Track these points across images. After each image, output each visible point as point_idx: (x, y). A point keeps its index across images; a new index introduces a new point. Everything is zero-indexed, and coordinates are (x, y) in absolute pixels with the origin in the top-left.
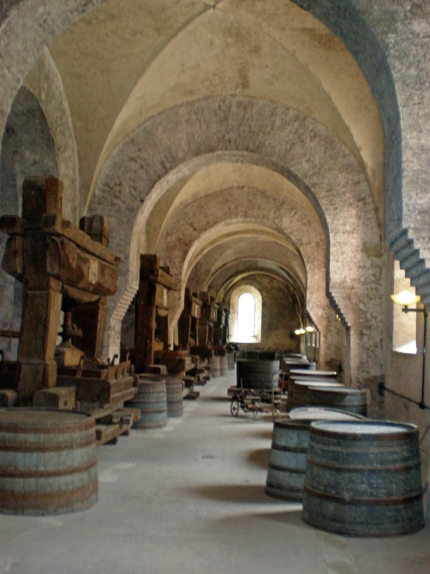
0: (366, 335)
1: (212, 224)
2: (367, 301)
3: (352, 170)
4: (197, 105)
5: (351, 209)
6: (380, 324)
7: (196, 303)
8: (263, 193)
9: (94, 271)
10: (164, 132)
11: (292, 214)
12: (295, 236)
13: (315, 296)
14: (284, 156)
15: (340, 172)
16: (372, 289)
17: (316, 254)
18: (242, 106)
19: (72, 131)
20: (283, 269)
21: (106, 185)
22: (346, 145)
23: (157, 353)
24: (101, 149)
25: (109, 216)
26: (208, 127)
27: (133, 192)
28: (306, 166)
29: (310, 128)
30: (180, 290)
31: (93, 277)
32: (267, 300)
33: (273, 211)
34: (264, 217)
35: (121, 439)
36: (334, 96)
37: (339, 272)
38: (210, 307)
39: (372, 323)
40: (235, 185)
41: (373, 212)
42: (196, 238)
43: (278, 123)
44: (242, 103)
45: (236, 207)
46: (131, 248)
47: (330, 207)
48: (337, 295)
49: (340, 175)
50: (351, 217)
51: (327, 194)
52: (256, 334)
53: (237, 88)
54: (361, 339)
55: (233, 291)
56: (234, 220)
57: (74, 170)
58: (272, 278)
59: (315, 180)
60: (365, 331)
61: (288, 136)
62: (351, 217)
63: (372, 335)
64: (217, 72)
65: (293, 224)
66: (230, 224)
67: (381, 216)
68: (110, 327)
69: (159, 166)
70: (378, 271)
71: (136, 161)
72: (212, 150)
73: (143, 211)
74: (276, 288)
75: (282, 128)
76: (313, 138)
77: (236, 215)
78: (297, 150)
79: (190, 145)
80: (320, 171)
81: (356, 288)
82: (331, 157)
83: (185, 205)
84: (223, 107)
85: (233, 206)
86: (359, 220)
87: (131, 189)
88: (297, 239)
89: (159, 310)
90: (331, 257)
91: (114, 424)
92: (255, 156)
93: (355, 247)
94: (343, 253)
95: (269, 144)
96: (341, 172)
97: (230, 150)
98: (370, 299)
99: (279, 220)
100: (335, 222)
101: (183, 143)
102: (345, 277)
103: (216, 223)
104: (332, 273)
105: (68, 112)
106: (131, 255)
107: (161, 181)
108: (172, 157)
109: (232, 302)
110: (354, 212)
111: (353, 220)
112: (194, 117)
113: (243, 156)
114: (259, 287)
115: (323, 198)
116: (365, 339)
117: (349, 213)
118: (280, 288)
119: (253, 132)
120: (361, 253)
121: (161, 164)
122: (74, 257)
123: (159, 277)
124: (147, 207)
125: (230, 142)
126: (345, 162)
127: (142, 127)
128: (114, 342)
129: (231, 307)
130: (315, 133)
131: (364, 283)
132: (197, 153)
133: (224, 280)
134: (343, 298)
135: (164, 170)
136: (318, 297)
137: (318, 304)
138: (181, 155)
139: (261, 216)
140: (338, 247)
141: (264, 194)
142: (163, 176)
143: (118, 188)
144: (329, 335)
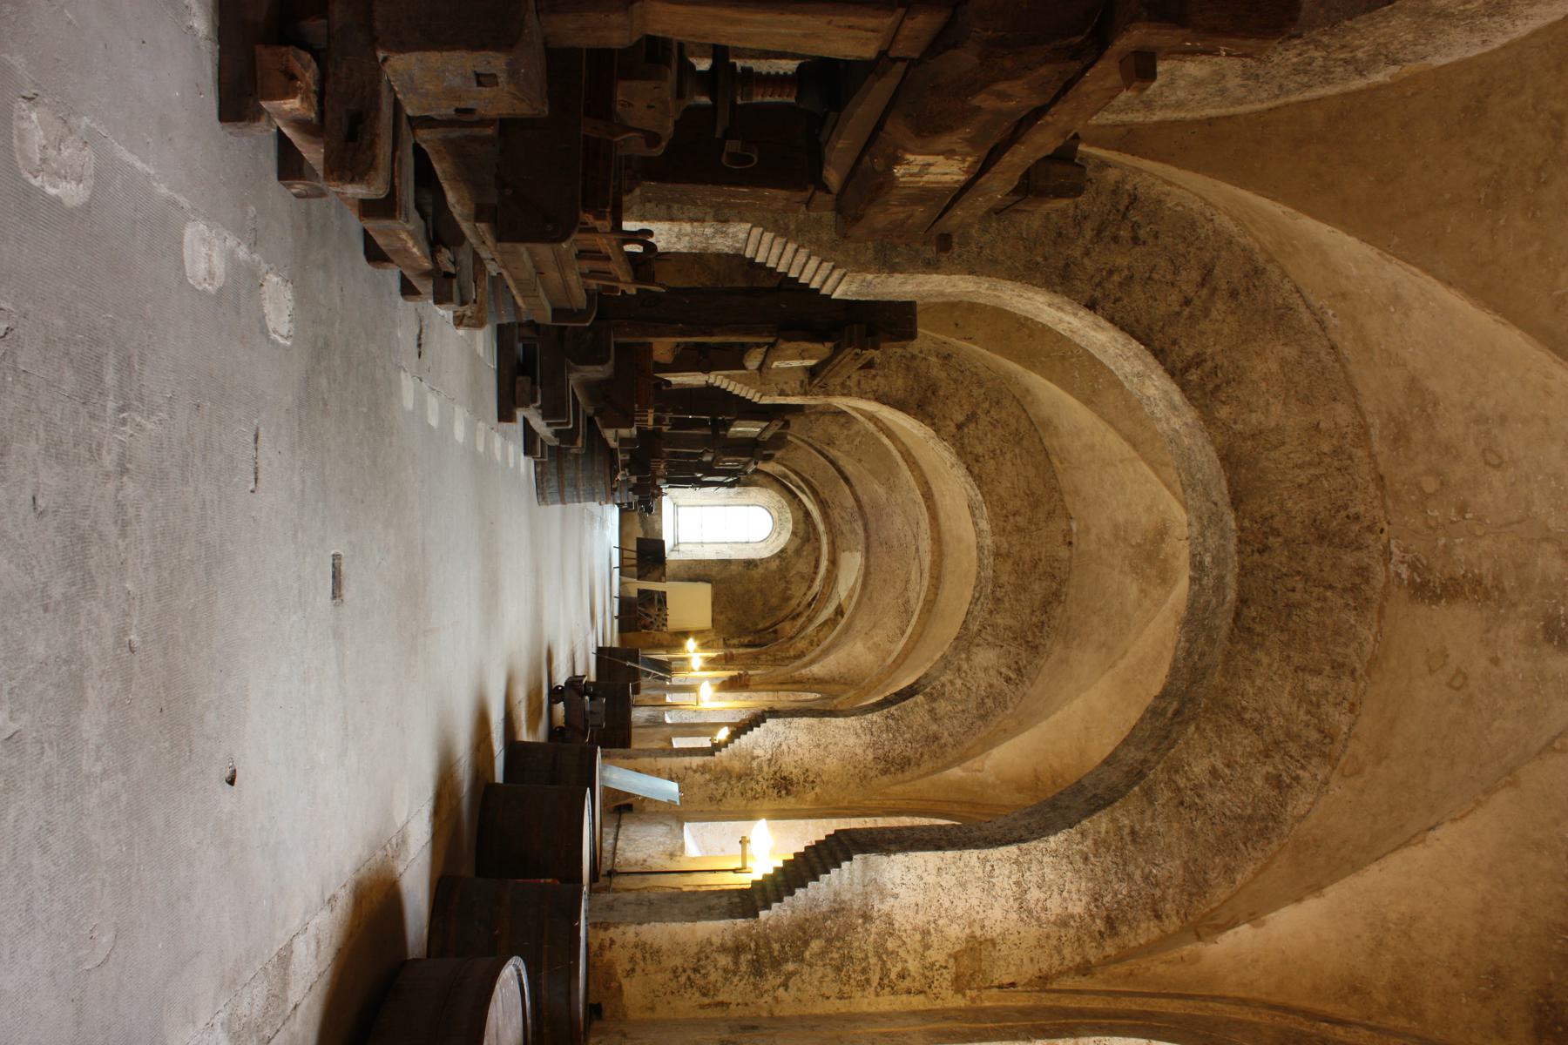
0: (736, 963)
1: (976, 470)
2: (832, 959)
3: (1191, 895)
4: (1360, 453)
5: (1085, 899)
6: (766, 998)
7: (764, 430)
8: (1057, 594)
9: (932, 169)
10: (1283, 362)
12: (952, 683)
13: (804, 738)
14: (1227, 706)
15: (1186, 863)
16: (864, 971)
17: (907, 736)
18: (1358, 580)
19: (1293, 98)
20: (839, 611)
21: (1134, 199)
22: (1256, 874)
23: (648, 349)
24: (1242, 185)
26: (1300, 486)
27: (1116, 278)
28: (1199, 769)
29: (1301, 772)
30: (805, 394)
31: (915, 170)
32: (761, 570)
33: (1012, 622)
34: (998, 600)
35: (390, 277)
36: (1419, 854)
37: (912, 876)
39: (770, 977)
40: (1074, 526)
41: (1078, 959)
42: (937, 431)
43: (1315, 684)
44: (1367, 581)
46: (956, 278)
47: (1089, 842)
48: (846, 875)
49: (1178, 862)
50: (1065, 900)
51: (1127, 830)
52: (681, 547)
53: (1413, 567)
54: (723, 949)
56: (984, 525)
57: (1180, 105)
58: (813, 581)
59: (1163, 795)
60: (745, 958)
61: (1280, 713)
62: (1065, 900)
63: (736, 980)
64: (1468, 516)
65: (982, 675)
66: (973, 515)
67: (1069, 983)
68: (726, 221)
69: (1190, 352)
70: (917, 984)
71: (1203, 284)
72: (1236, 502)
73: (1059, 309)
74: (790, 589)
75: (1302, 696)
76: (1275, 781)
77: (999, 531)
78: (1243, 742)
79: (1253, 436)
80: (1190, 807)
81: (867, 925)
82: (1226, 834)
83: (1021, 400)
84: (1355, 527)
86: (1055, 923)
87: (1126, 272)
88: (943, 685)
89: (763, 350)
90: (949, 854)
91: (433, 255)
92: (1224, 623)
93: (982, 915)
94: (963, 885)
95: (1258, 663)
96: (1185, 865)
97: (1239, 552)
98: (838, 969)
99: (990, 639)
100: (1047, 859)
101: (1254, 418)
102: (896, 896)
103: (978, 479)
104: (907, 859)
105: (1357, 84)
106: (936, 278)
107: (1150, 359)
108: (1218, 387)
109: (754, 492)
110: (1077, 908)
111: (1055, 905)
112: (1326, 448)
113: (1219, 586)
114: (790, 552)
115: (1113, 820)
116: (724, 961)
117: (1075, 897)
118: (789, 599)
119: (1289, 615)
120: (963, 936)
121: (1198, 355)
122: (1009, 97)
123: (858, 351)
124: (1068, 318)
125: (1260, 552)
126: (1212, 875)
127: (1294, 299)
128: (679, 237)
130: (1289, 787)
131: (881, 951)
132: (1229, 459)
134: (837, 894)
135: (1179, 365)
136: (800, 745)
137: (784, 747)
138: (1223, 412)
140: (980, 871)
141: (1054, 598)
142: (1163, 362)
143: (1124, 234)
144: (708, 776)
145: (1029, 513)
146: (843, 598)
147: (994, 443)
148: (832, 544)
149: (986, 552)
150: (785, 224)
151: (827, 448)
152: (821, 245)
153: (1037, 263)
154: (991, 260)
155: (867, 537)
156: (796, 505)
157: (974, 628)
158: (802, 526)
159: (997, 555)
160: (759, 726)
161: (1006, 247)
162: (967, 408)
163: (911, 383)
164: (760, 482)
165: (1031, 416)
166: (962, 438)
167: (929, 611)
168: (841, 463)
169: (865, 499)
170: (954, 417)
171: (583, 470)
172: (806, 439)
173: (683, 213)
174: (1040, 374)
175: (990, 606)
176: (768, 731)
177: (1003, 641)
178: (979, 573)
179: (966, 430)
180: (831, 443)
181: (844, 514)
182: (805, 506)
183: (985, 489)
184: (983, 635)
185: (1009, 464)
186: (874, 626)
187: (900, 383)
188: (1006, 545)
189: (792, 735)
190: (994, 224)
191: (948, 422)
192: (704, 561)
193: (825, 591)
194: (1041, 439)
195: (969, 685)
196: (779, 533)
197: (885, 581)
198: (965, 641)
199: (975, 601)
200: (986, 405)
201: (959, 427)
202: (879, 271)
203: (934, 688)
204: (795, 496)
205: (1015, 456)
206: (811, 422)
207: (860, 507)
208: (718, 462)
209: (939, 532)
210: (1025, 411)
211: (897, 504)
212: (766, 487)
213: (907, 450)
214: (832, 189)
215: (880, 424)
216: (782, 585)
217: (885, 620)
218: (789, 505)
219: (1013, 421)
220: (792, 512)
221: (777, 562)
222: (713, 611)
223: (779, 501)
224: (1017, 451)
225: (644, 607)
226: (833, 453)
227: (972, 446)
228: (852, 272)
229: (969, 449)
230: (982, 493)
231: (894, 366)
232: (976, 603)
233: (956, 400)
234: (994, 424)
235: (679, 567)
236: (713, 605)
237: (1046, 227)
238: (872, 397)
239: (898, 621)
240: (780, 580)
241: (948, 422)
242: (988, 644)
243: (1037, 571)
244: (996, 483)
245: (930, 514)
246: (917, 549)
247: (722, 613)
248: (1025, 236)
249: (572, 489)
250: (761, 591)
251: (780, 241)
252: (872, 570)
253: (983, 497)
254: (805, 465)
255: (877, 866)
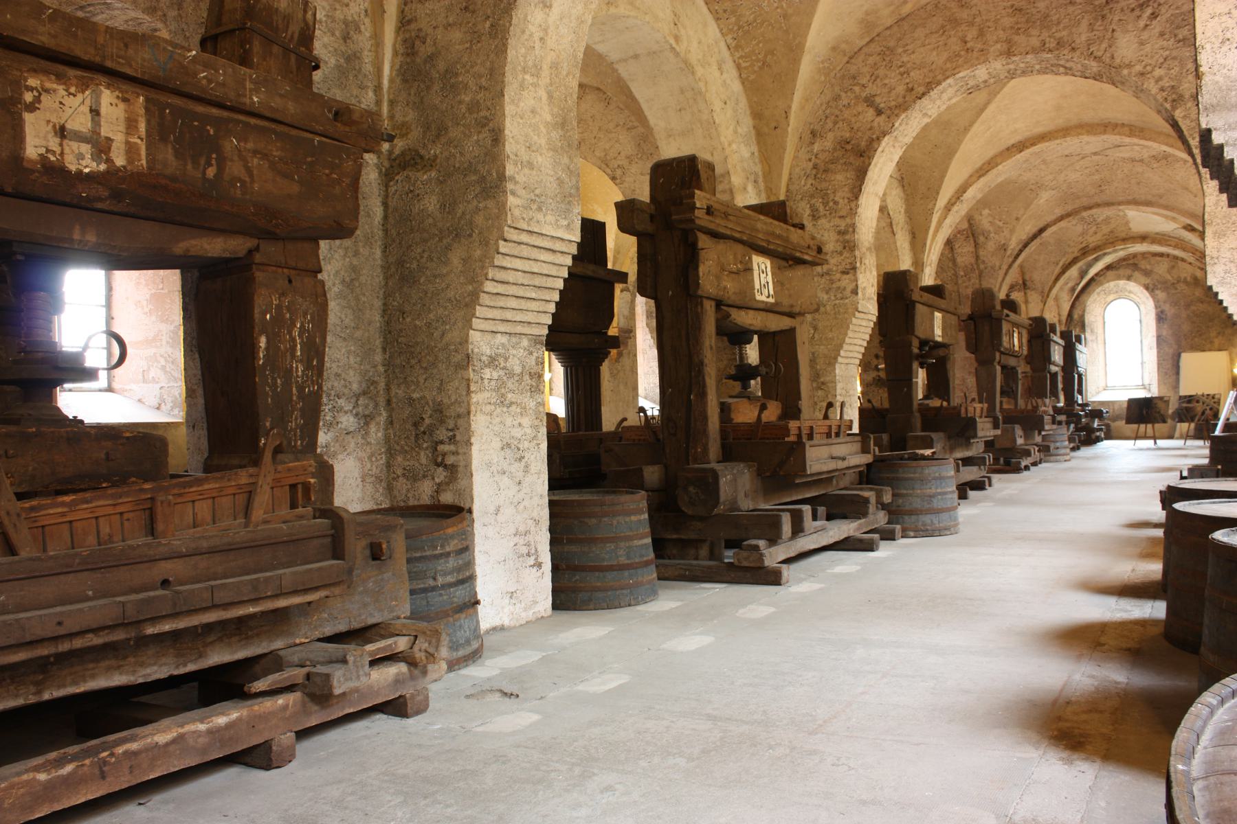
1: (921, 89)
11: (1142, 23)
25: (448, 26)
32: (1167, 307)
34: (1060, 44)
38: (999, 321)
42: (884, 134)
45: (981, 33)
52: (1146, 383)
55: (1090, 294)
58: (1176, 258)
74: (1185, 278)
85: (972, 33)
99: (1104, 45)
103: (930, 86)
106: (512, 129)
109: (1089, 318)
114: (1148, 281)
129: (1088, 330)
133: (1057, 270)
139: (1052, 44)
145: (963, 27)
146: (1176, 226)
147: (893, 75)
148: (1126, 239)
149: (1012, 66)
150: (469, 295)
151: (1009, 252)
152: (485, 256)
153: (492, 25)
154: (491, 75)
155: (1098, 205)
156: (1102, 278)
157: (1094, 66)
158: (1121, 272)
159: (1009, 53)
160: (1217, 294)
161: (479, 61)
162: (861, 107)
163: (839, 167)
164: (1080, 313)
165: (864, 42)
166: (890, 108)
167: (1142, 130)
168: (1024, 237)
169: (1059, 212)
170: (870, 119)
171: (913, 489)
172: (1003, 271)
173: (463, 402)
174: (806, 37)
175: (1066, 52)
176: (1222, 283)
177: (1106, 29)
178: (1039, 72)
179: (882, 105)
180: (1004, 248)
181: (1091, 231)
182: (1102, 270)
183: (940, 77)
184: (1100, 54)
185: (912, 56)
186: (1187, 189)
187: (840, 177)
188: (999, 46)
189: (1228, 255)
190: (461, 79)
191: (875, 124)
192: (1158, 361)
193: (1173, 244)
194: (887, 28)
195: (1161, 60)
196: (1130, 292)
197: (1138, 184)
198: (1110, 73)
199: (1068, 71)
200: (857, 89)
201: (879, 112)
202: (505, 192)
203: (1166, 99)
204: (1092, 280)
205: (905, 51)
206: (986, 268)
207: (1068, 215)
208: (1014, 351)
209: (1057, 131)
210: (860, 49)
211: (1055, 179)
212: (1085, 306)
213: (977, 171)
214: (256, 245)
215: (954, 200)
216: (1181, 286)
217: (1178, 178)
218: (1102, 284)
219: (871, 60)
220: (1108, 282)
221: (1158, 292)
222: (1210, 350)
223: (1098, 294)
224: (900, 50)
225: (1195, 416)
226: (1014, 245)
227: (898, 96)
228: (506, 221)
229: (901, 100)
230: (944, 80)
231: (824, 185)
232: (1070, 69)
233: (853, 120)
234: (874, 78)
235: (1165, 384)
236: (1204, 351)
237: (460, 25)
238: (855, 202)
239: (1178, 165)
240: (1176, 289)
241: (875, 124)
242: (1110, 47)
243: (1024, 7)
244: (934, 66)
245: (1039, 142)
246: (1095, 154)
247: (1211, 342)
248: (468, 45)
249: (935, 501)
250: (1188, 306)
251: (484, 299)
252: (1130, 198)
253: (948, 78)
254: (1047, 272)
255: (1220, 89)
